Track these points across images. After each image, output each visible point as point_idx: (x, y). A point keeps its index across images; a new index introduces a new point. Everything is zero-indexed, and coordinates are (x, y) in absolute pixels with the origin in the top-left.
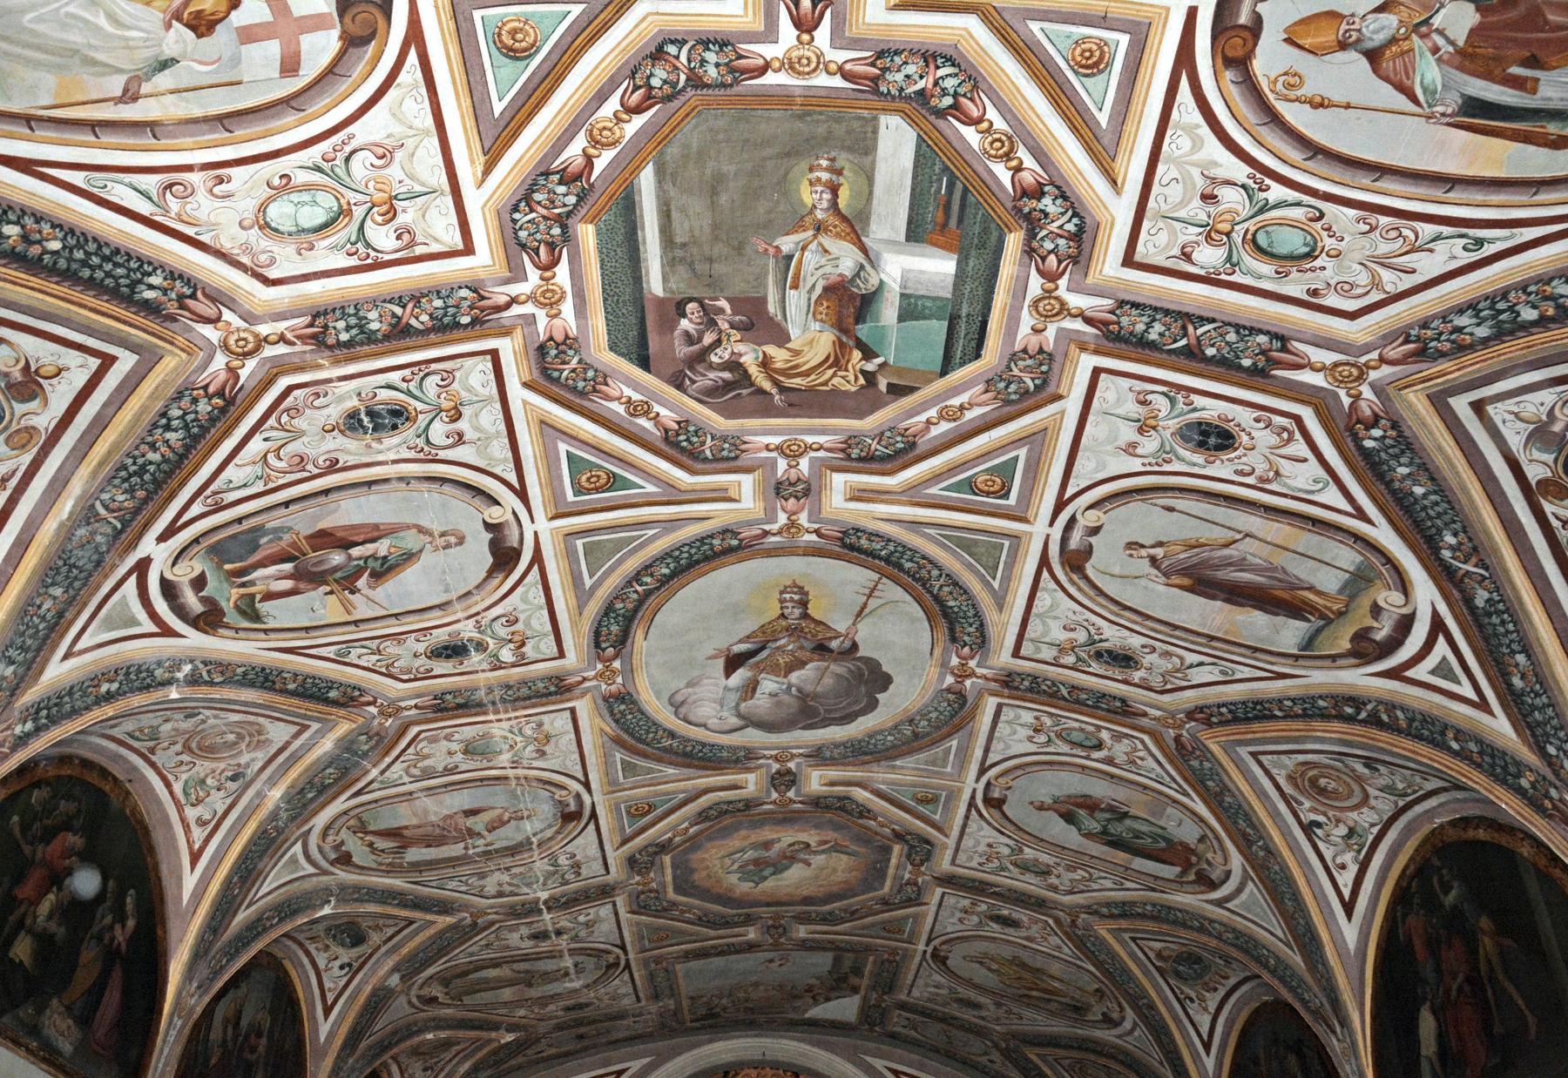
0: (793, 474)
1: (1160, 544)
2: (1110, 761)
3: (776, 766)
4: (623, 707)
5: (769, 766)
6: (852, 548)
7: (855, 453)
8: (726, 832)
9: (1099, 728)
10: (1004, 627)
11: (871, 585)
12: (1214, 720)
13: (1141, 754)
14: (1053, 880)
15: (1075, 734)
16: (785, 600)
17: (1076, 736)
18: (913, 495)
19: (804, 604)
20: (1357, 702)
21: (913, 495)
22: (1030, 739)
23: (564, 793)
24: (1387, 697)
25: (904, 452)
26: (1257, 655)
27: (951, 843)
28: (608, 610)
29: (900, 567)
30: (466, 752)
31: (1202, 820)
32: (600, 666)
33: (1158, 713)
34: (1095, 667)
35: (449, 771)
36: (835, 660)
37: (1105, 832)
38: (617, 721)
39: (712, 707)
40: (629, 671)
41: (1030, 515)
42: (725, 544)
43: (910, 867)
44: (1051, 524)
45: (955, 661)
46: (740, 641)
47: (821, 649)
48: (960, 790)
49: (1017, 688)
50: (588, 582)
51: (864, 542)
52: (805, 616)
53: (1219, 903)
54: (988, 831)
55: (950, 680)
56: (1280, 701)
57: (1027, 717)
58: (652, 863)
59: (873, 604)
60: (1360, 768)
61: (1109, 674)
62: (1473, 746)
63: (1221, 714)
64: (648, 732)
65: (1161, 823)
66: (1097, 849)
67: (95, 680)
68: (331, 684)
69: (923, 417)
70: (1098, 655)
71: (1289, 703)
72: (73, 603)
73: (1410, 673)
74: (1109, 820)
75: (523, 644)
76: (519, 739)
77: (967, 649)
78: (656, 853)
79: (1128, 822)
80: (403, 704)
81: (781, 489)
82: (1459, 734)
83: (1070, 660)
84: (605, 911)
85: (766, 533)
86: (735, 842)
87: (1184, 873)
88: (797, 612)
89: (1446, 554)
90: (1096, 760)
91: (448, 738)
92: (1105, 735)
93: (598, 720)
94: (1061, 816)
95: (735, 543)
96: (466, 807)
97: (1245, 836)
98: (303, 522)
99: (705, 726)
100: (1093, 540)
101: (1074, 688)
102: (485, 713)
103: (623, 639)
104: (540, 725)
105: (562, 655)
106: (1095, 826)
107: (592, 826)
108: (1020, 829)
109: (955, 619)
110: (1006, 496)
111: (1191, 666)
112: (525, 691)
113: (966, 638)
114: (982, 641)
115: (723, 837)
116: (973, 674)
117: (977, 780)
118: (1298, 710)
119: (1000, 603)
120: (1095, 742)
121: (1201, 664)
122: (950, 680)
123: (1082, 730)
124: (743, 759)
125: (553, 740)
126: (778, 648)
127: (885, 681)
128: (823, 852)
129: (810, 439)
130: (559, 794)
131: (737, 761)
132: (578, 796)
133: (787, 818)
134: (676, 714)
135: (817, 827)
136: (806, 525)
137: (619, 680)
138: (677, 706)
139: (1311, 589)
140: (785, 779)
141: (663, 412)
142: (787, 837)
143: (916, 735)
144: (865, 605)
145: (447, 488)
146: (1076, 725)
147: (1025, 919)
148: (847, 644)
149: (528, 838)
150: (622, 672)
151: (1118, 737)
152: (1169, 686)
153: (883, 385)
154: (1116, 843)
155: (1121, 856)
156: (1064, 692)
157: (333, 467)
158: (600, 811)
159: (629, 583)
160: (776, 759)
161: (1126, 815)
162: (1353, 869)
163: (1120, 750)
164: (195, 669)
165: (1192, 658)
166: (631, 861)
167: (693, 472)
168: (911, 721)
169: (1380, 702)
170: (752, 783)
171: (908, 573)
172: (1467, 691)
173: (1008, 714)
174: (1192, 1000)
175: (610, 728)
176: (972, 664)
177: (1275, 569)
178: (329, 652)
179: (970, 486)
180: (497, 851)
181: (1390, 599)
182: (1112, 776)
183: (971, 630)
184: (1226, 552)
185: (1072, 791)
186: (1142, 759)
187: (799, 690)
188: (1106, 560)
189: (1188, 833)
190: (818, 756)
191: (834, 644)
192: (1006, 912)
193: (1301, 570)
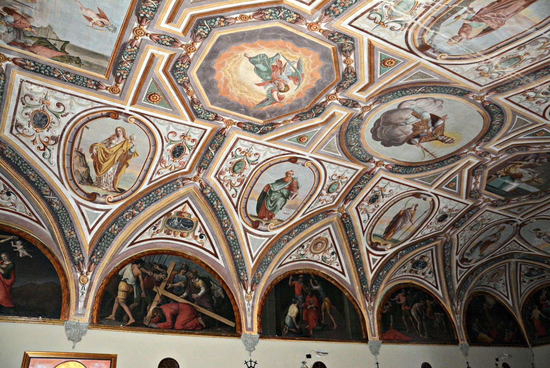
2: (320, 194)
9: (339, 193)
13: (325, 203)
17: (335, 187)
20: (357, 246)
24: (361, 252)
26: (372, 227)
27: (263, 141)
30: (519, 57)
34: (370, 194)
37: (271, 192)
43: (238, 121)
49: (365, 174)
53: (246, 231)
55: (377, 160)
60: (331, 251)
62: (362, 273)
65: (284, 208)
66: (258, 190)
73: (370, 254)
79: (282, 199)
82: (363, 270)
87: (255, 217)
92: (335, 194)
96: (494, 33)
97: (291, 232)
132: (435, 58)
146: (341, 187)
149: (436, 30)
161: (286, 198)
162: (291, 260)
169: (359, 251)
172: (373, 267)
174: (155, 228)
180: (448, 16)
181: (389, 246)
182: (311, 196)
192: (187, 152)
193: (400, 232)
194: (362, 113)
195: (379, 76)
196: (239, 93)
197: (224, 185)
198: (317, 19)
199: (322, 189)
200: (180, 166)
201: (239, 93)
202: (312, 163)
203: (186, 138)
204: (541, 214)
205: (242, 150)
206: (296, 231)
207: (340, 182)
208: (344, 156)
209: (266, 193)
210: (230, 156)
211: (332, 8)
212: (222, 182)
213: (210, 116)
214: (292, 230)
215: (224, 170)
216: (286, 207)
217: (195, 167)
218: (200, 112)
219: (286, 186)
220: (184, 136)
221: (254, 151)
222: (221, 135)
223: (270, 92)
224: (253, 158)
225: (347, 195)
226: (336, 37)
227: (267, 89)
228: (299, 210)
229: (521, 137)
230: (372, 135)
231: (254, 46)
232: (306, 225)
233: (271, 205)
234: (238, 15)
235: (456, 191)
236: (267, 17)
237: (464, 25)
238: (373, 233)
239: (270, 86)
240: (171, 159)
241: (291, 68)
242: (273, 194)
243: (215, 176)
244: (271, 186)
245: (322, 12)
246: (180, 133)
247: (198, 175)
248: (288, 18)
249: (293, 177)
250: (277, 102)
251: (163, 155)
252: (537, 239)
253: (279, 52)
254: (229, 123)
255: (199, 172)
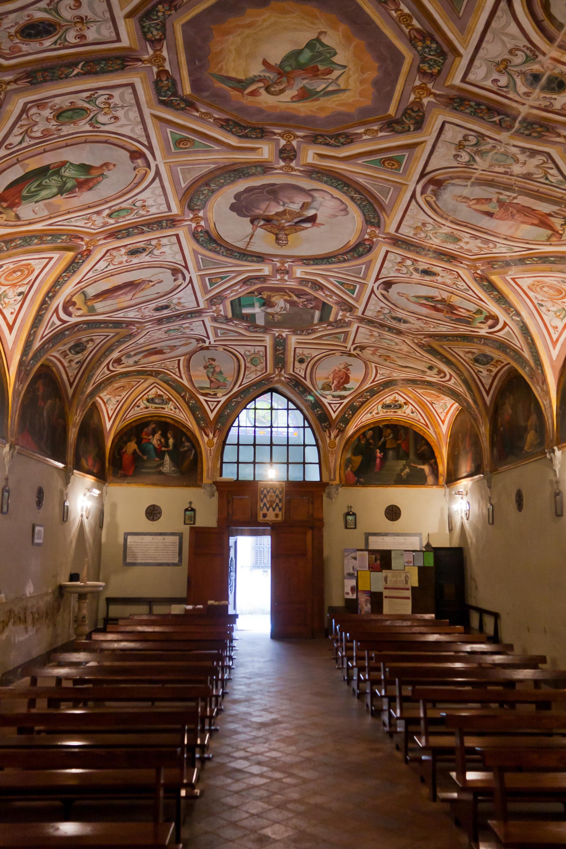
0: (282, 275)
1: (153, 286)
3: (293, 164)
4: (373, 220)
5: (296, 165)
6: (259, 257)
7: (262, 279)
8: (339, 118)
9: (117, 222)
10: (188, 245)
11: (249, 246)
12: (79, 256)
14: (47, 113)
15: (126, 214)
16: (286, 241)
18: (240, 273)
19: (277, 239)
21: (240, 273)
22: (144, 201)
23: (428, 199)
25: (245, 282)
27: (147, 112)
28: (360, 256)
29: (238, 253)
31: (30, 224)
32: (375, 240)
33: (100, 242)
34: (142, 245)
35: (476, 237)
36: (261, 215)
37: (57, 172)
38: (379, 216)
39: (327, 203)
40: (363, 231)
41: (199, 277)
42: (308, 261)
43: (167, 67)
44: (190, 277)
45: (202, 223)
46: (307, 228)
47: (268, 220)
48: (164, 157)
50: (364, 267)
51: (255, 259)
52: (276, 235)
54: (126, 131)
56: (69, 277)
57: (153, 210)
58: (405, 113)
59: (247, 239)
61: (134, 245)
63: (80, 259)
64: (365, 206)
67: (528, 344)
68: (482, 286)
69: (242, 289)
70: (144, 250)
71: (66, 279)
72: (508, 347)
74: (65, 183)
75: (400, 263)
76: (431, 235)
77: (199, 230)
78: (398, 122)
79: (55, 190)
80: (466, 267)
81: (287, 272)
83: (154, 242)
84: (479, 74)
85: (292, 262)
86: (331, 104)
88: (280, 236)
89: (82, 325)
90: (104, 210)
91: (462, 248)
92: (112, 221)
93: (388, 221)
94: (92, 166)
95: (305, 261)
97: (12, 241)
98: (440, 315)
99: (333, 197)
100: (174, 278)
101: (142, 232)
102: (436, 248)
103: (360, 244)
104: (415, 234)
105: (387, 252)
106: (67, 173)
107: (428, 169)
108: (106, 142)
109: (209, 239)
110: (209, 279)
111: (109, 265)
112: (412, 248)
113: (202, 235)
114: (195, 235)
115: (340, 114)
116: (191, 220)
117: (157, 166)
118: (61, 280)
119: (195, 252)
120: (113, 216)
121: (106, 267)
122: (201, 214)
123: (124, 217)
124: (313, 172)
125: (415, 226)
126: (289, 222)
127: (233, 208)
128: (253, 81)
129: (277, 282)
130: (432, 200)
131: (318, 172)
132: (422, 193)
133: (288, 121)
134: (347, 207)
135: (260, 111)
136: (277, 263)
137: (369, 231)
138: (345, 210)
139: (101, 301)
140: (288, 154)
141: (322, 294)
142: (284, 100)
143: (207, 185)
144: (251, 239)
145: (393, 302)
146: (128, 218)
147: (24, 48)
148: (256, 223)
150: (366, 233)
151: (105, 224)
152: (108, 254)
153: (256, 293)
154: (43, 172)
155: (33, 164)
156: (145, 229)
157: (419, 319)
158: (416, 176)
159: (348, 260)
160: (293, 169)
161: (61, 191)
163: (99, 220)
164: (513, 315)
165: (111, 267)
166: (419, 124)
167: (316, 280)
168: (213, 192)
170: (310, 155)
171: (235, 252)
173: (164, 208)
175: (383, 216)
176: (194, 225)
177: (115, 298)
178: (470, 292)
179: (222, 278)
182: (89, 207)
183: (201, 239)
184: (133, 293)
185: (99, 186)
186: (86, 223)
187: (278, 203)
188: (167, 276)
189: (26, 210)
190: (265, 168)
191: (262, 223)
192: (48, 43)
194: (276, 169)
195: (360, 162)
196: (232, 48)
197: (20, 123)
198: (438, 92)
199: (110, 208)
200: (7, 51)
201: (232, 48)
202: (145, 174)
203: (79, 26)
204: (233, 347)
205: (110, 101)
206: (20, 241)
207: (136, 211)
208: (184, 190)
209: (50, 170)
210: (87, 94)
211: (467, 103)
212: (24, 116)
213: (155, 33)
214: (15, 239)
215: (50, 105)
216: (45, 205)
217: (22, 70)
218: (155, 17)
219: (83, 178)
220: (82, 20)
221: (120, 113)
222: (121, 64)
223: (257, 79)
224: (102, 118)
225: (120, 231)
226: (414, 114)
227: (262, 74)
228: (52, 216)
229: (331, 279)
230: (243, 190)
231: (348, 39)
232: (36, 241)
233: (33, 189)
234: (406, 11)
235: (209, 288)
236: (420, 44)
237: (489, 200)
238: (84, 289)
239: (272, 76)
240: (12, 31)
241: (324, 86)
242: (54, 178)
243: (26, 104)
244: (67, 165)
245: (455, 95)
246: (84, 11)
247: (9, 83)
248: (427, 65)
249: (105, 173)
250: (242, 93)
251: (12, 16)
252: (202, 368)
253: (350, 66)
254: (157, 59)
255: (15, 81)
